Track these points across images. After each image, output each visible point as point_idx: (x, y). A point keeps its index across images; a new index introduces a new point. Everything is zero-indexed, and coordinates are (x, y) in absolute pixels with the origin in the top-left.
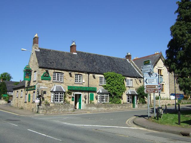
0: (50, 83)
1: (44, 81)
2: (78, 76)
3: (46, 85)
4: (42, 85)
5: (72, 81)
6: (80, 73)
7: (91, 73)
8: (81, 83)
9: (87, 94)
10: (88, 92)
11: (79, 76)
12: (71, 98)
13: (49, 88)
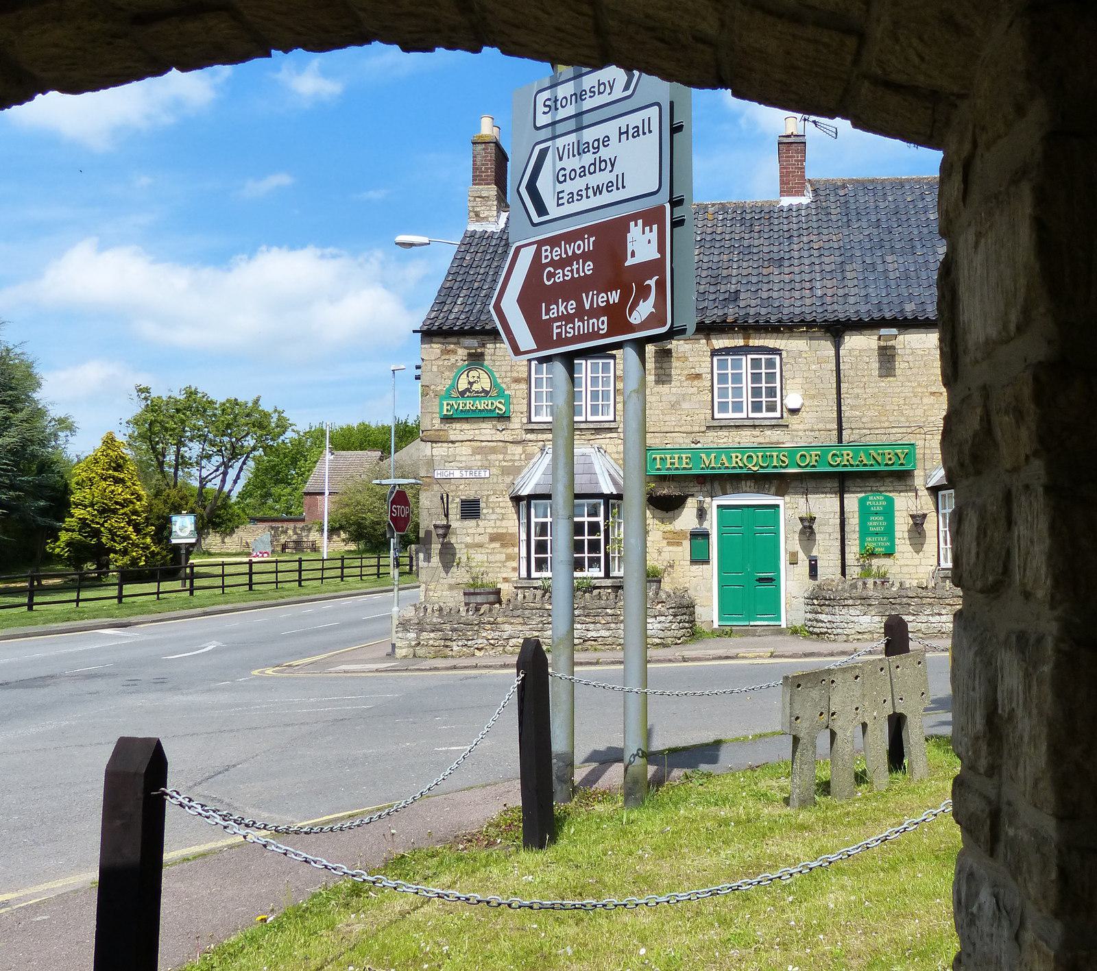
0: (506, 436)
1: (466, 426)
2: (746, 360)
3: (475, 452)
4: (447, 460)
5: (685, 405)
6: (755, 342)
7: (859, 326)
8: (778, 414)
9: (824, 505)
10: (842, 481)
11: (756, 364)
12: (687, 544)
13: (505, 471)
